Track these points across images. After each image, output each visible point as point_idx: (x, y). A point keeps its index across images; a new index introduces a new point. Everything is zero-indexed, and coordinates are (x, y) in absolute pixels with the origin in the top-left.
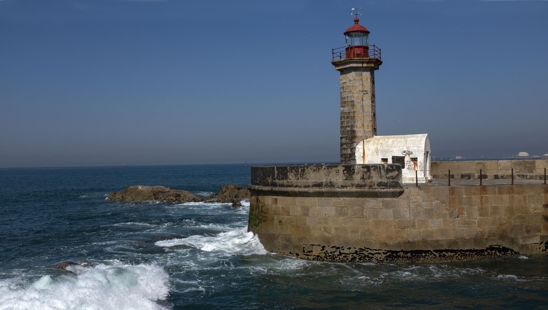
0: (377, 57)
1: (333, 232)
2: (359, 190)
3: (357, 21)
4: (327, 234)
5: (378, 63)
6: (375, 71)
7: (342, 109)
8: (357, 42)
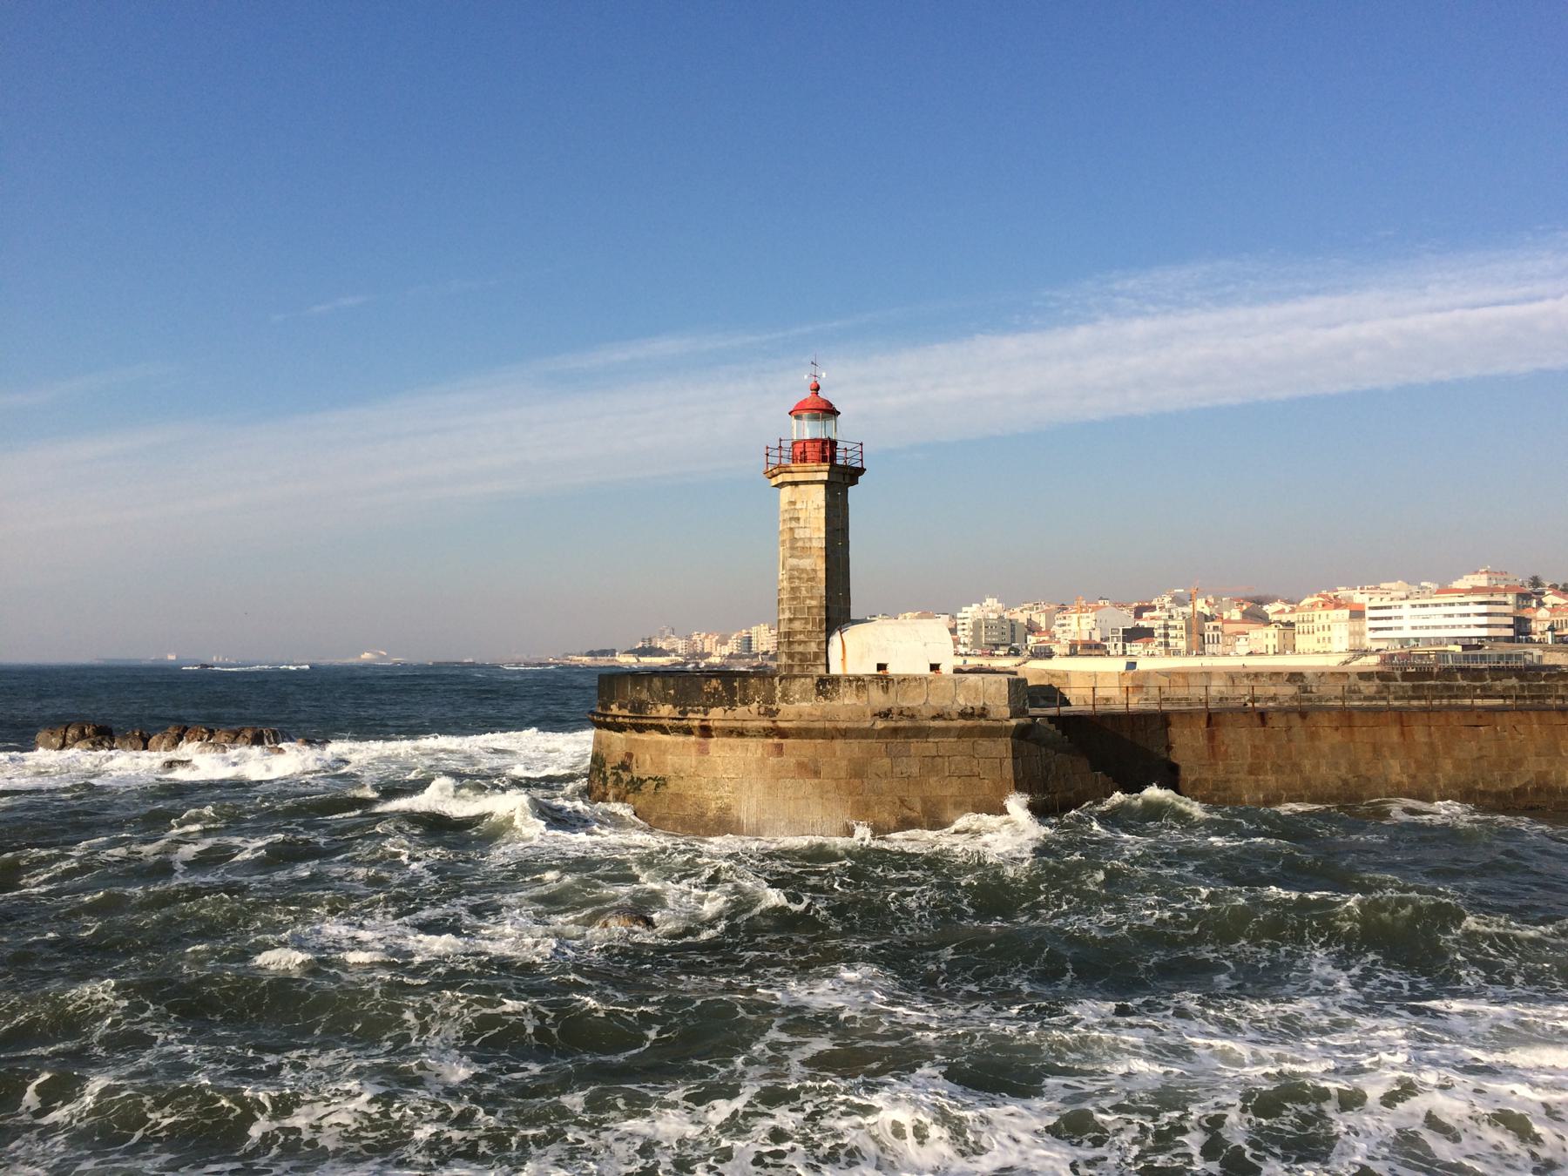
1: (918, 808)
2: (969, 723)
4: (906, 812)
7: (794, 561)
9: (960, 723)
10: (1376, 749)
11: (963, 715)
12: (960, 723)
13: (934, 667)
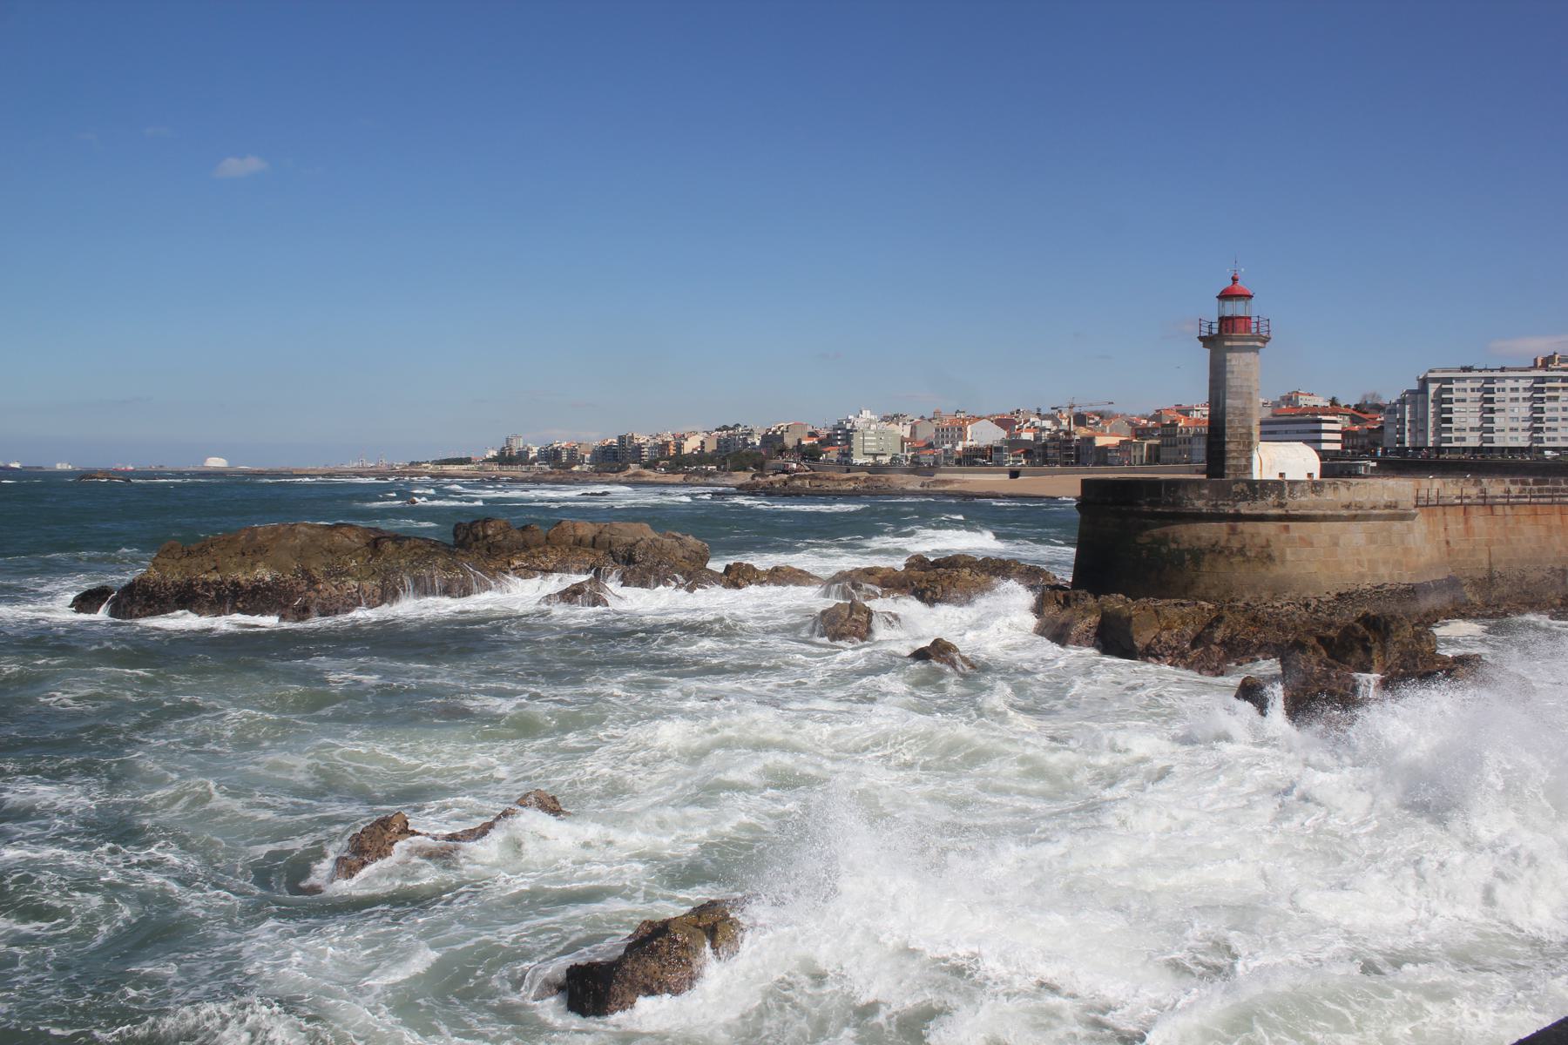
8: (1234, 308)
9: (1387, 511)
10: (1549, 528)
11: (1387, 507)
12: (1387, 511)
13: (1310, 475)
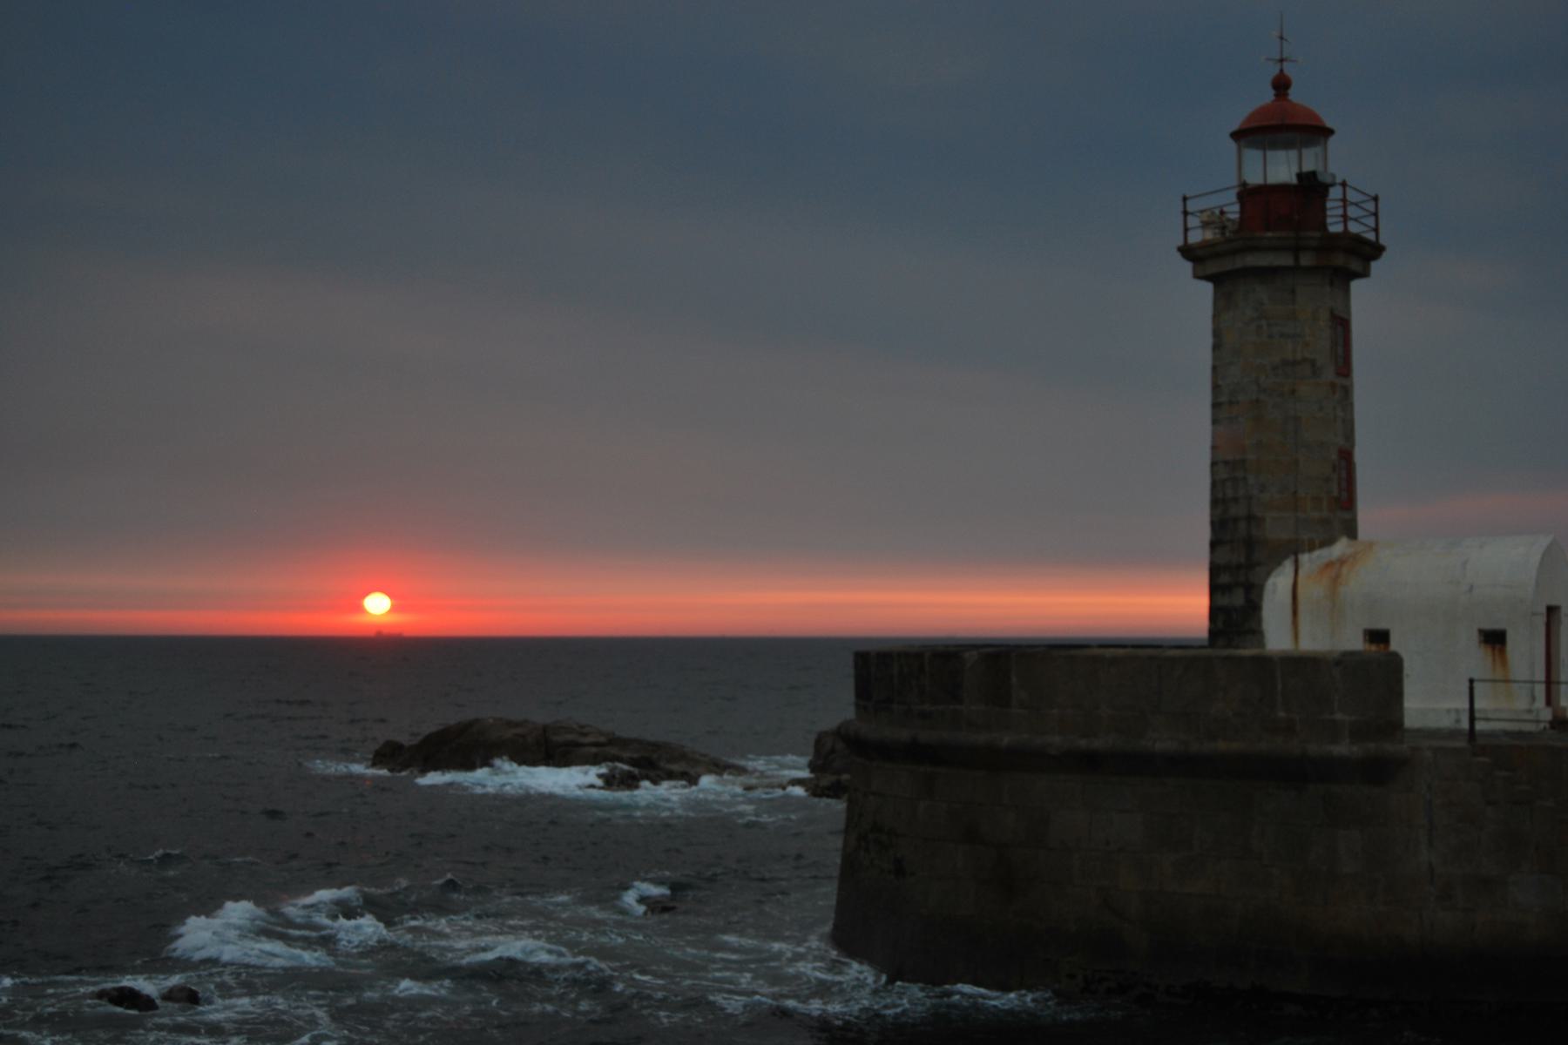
0: (1354, 228)
3: (1281, 85)
5: (1366, 252)
6: (1356, 286)
8: (1281, 168)
